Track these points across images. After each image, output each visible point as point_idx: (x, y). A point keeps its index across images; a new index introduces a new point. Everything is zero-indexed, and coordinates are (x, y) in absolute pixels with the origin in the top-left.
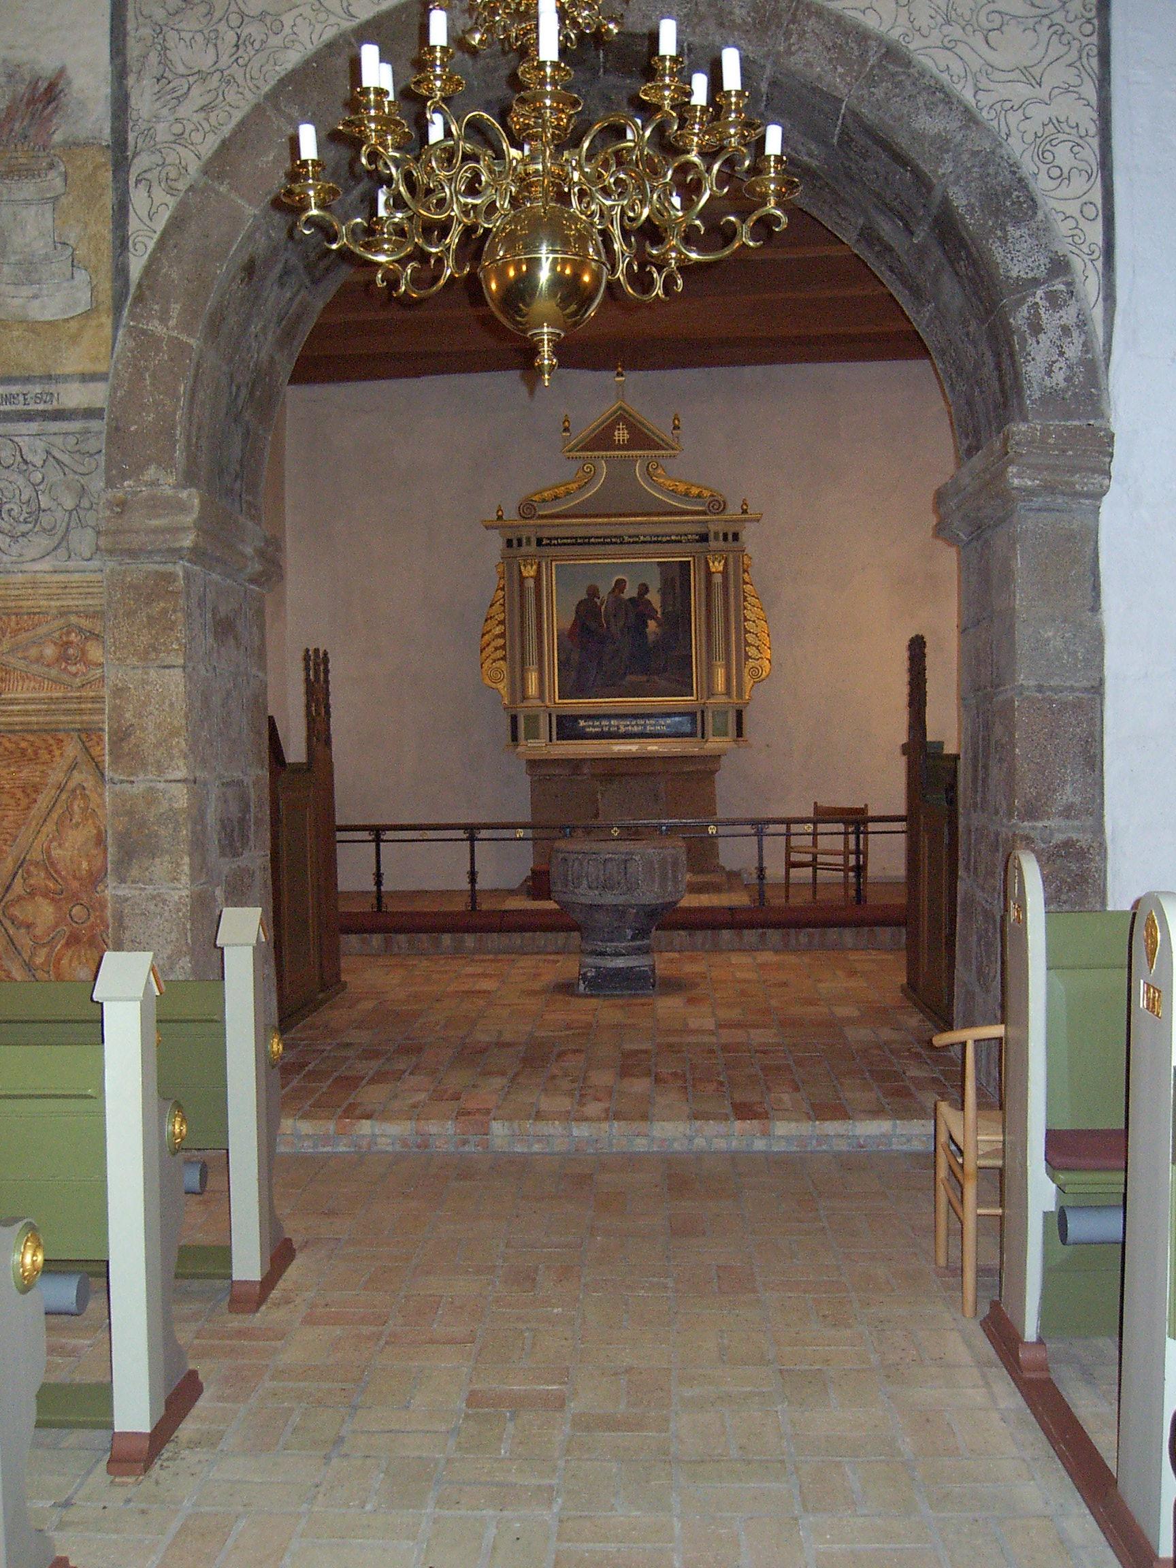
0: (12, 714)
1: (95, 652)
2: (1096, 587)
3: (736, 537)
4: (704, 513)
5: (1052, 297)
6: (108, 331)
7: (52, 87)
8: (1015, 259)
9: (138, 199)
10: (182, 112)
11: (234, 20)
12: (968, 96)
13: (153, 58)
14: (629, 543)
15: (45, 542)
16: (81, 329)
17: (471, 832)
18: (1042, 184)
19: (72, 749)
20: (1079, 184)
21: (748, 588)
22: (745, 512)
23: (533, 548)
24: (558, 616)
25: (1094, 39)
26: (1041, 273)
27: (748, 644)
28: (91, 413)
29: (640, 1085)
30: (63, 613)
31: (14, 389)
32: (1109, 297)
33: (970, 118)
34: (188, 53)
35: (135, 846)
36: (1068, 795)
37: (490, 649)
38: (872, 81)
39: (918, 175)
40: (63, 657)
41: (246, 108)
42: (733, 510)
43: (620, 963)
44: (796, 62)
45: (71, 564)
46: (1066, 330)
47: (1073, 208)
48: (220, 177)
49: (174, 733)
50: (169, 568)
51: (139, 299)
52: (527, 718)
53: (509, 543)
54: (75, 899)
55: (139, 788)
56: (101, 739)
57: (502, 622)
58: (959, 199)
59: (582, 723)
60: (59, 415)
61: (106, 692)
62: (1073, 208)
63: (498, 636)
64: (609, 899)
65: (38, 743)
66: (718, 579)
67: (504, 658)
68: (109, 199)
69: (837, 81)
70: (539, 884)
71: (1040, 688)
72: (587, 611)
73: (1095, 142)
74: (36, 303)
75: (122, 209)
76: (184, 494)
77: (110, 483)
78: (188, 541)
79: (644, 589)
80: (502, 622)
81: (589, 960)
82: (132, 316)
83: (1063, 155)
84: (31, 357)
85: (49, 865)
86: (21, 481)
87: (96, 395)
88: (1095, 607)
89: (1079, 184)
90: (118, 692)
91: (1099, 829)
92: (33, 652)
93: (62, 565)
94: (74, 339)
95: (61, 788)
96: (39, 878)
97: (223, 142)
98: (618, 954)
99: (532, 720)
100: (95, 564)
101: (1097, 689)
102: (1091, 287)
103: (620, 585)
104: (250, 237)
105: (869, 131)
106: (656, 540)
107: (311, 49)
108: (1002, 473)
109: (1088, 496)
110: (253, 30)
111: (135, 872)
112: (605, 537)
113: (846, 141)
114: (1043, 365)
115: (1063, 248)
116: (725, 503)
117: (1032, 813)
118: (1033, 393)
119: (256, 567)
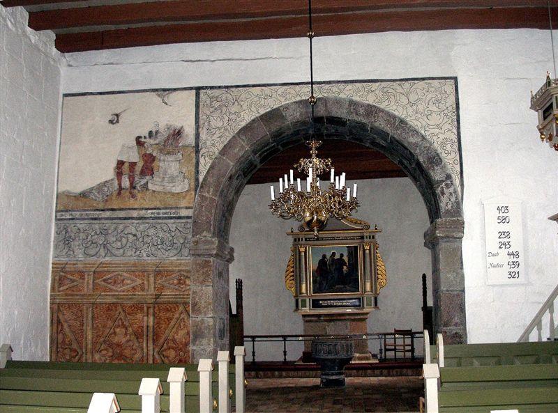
0: (165, 298)
1: (188, 282)
2: (462, 262)
3: (373, 237)
4: (362, 229)
5: (447, 185)
6: (193, 196)
7: (179, 131)
8: (437, 175)
9: (202, 160)
10: (214, 138)
11: (228, 114)
12: (423, 132)
13: (206, 124)
15: (175, 252)
16: (186, 195)
17: (285, 337)
18: (443, 155)
19: (181, 308)
20: (453, 154)
21: (378, 255)
22: (376, 229)
23: (304, 241)
24: (312, 264)
25: (455, 117)
26: (444, 179)
27: (378, 274)
28: (188, 217)
29: (339, 406)
30: (179, 271)
31: (168, 211)
32: (462, 185)
33: (423, 138)
34: (216, 123)
35: (198, 335)
36: (456, 320)
38: (397, 129)
39: (411, 153)
40: (179, 283)
41: (231, 137)
42: (372, 228)
43: (334, 377)
44: (377, 124)
45: (182, 258)
46: (451, 194)
47: (451, 161)
48: (224, 155)
49: (209, 304)
50: (208, 259)
51: (202, 187)
52: (302, 301)
53: (295, 240)
54: (181, 349)
55: (199, 319)
56: (189, 306)
57: (293, 267)
58: (421, 159)
59: (321, 302)
60: (180, 218)
61: (191, 293)
62: (451, 161)
63: (292, 272)
64: (330, 357)
65: (172, 307)
66: (367, 252)
67: (293, 280)
68: (194, 161)
69: (387, 129)
70: (307, 356)
71: (447, 291)
72: (322, 263)
73: (457, 144)
74: (174, 188)
75: (197, 163)
76: (214, 240)
77: (193, 236)
78: (215, 252)
79: (342, 255)
80: (293, 267)
81: (324, 377)
82: (200, 191)
83: (448, 147)
84: (172, 202)
85: (174, 340)
86: (169, 235)
87: (189, 213)
88: (462, 268)
89: (453, 154)
90: (194, 293)
91: (465, 329)
92: (171, 282)
93: (179, 258)
94: (184, 198)
95: (178, 319)
96: (171, 344)
97: (225, 146)
98: (333, 375)
99: (304, 302)
100: (189, 258)
101: (463, 291)
102: (457, 182)
103: (334, 254)
104: (232, 170)
105: (397, 141)
107: (248, 121)
108: (434, 233)
109: (458, 238)
110: (233, 117)
111: (197, 343)
113: (391, 142)
114: (445, 203)
115: (449, 172)
117: (446, 325)
118: (443, 211)
119: (228, 257)
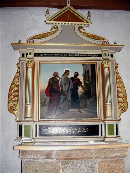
3: (112, 56)
14: (71, 56)
37: (12, 97)
53: (23, 55)
57: (18, 86)
66: (106, 70)
67: (17, 101)
72: (53, 82)
79: (77, 74)
80: (18, 86)
99: (28, 127)
103: (67, 72)
106: (82, 55)
112: (61, 54)
116: (108, 42)
